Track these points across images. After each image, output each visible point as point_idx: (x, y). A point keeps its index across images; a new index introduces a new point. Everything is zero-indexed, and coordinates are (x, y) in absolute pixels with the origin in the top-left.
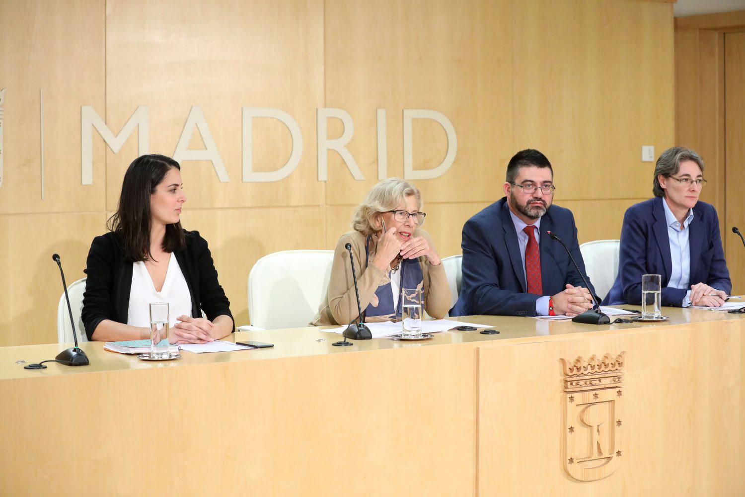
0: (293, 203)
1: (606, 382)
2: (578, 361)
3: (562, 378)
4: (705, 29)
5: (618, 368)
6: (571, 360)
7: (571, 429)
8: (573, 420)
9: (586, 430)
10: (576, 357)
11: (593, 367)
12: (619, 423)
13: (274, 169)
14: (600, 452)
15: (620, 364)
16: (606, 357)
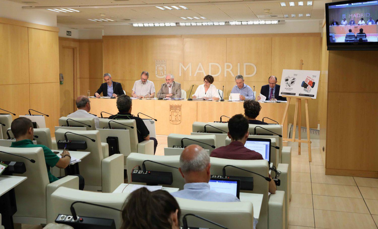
0: (219, 81)
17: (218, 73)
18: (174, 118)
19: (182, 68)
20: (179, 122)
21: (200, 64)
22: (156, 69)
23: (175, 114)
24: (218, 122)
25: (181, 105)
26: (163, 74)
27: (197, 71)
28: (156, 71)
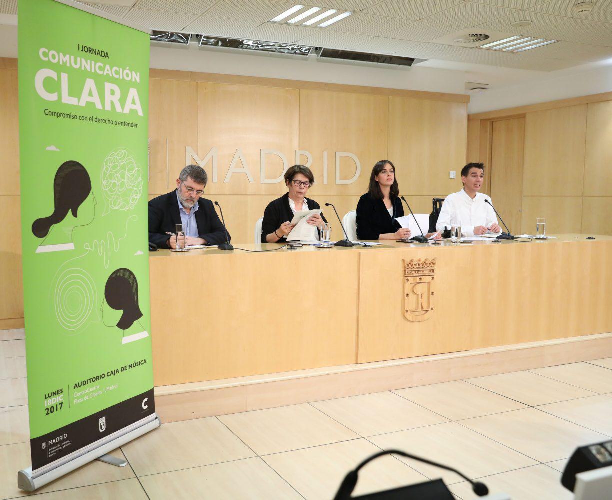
1: (426, 273)
2: (412, 261)
3: (403, 269)
4: (483, 120)
6: (408, 261)
7: (408, 295)
8: (408, 291)
9: (415, 296)
10: (411, 259)
11: (419, 265)
12: (433, 293)
14: (422, 308)
15: (434, 264)
16: (426, 260)
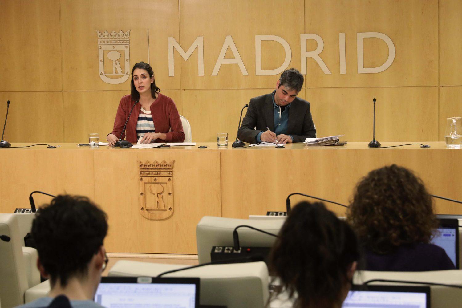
5: (169, 168)
9: (153, 195)
13: (275, 68)
17: (281, 65)
18: (151, 202)
19: (178, 57)
20: (169, 213)
21: (229, 41)
22: (101, 57)
23: (156, 188)
24: (281, 214)
25: (174, 161)
26: (120, 73)
27: (221, 60)
28: (101, 64)
